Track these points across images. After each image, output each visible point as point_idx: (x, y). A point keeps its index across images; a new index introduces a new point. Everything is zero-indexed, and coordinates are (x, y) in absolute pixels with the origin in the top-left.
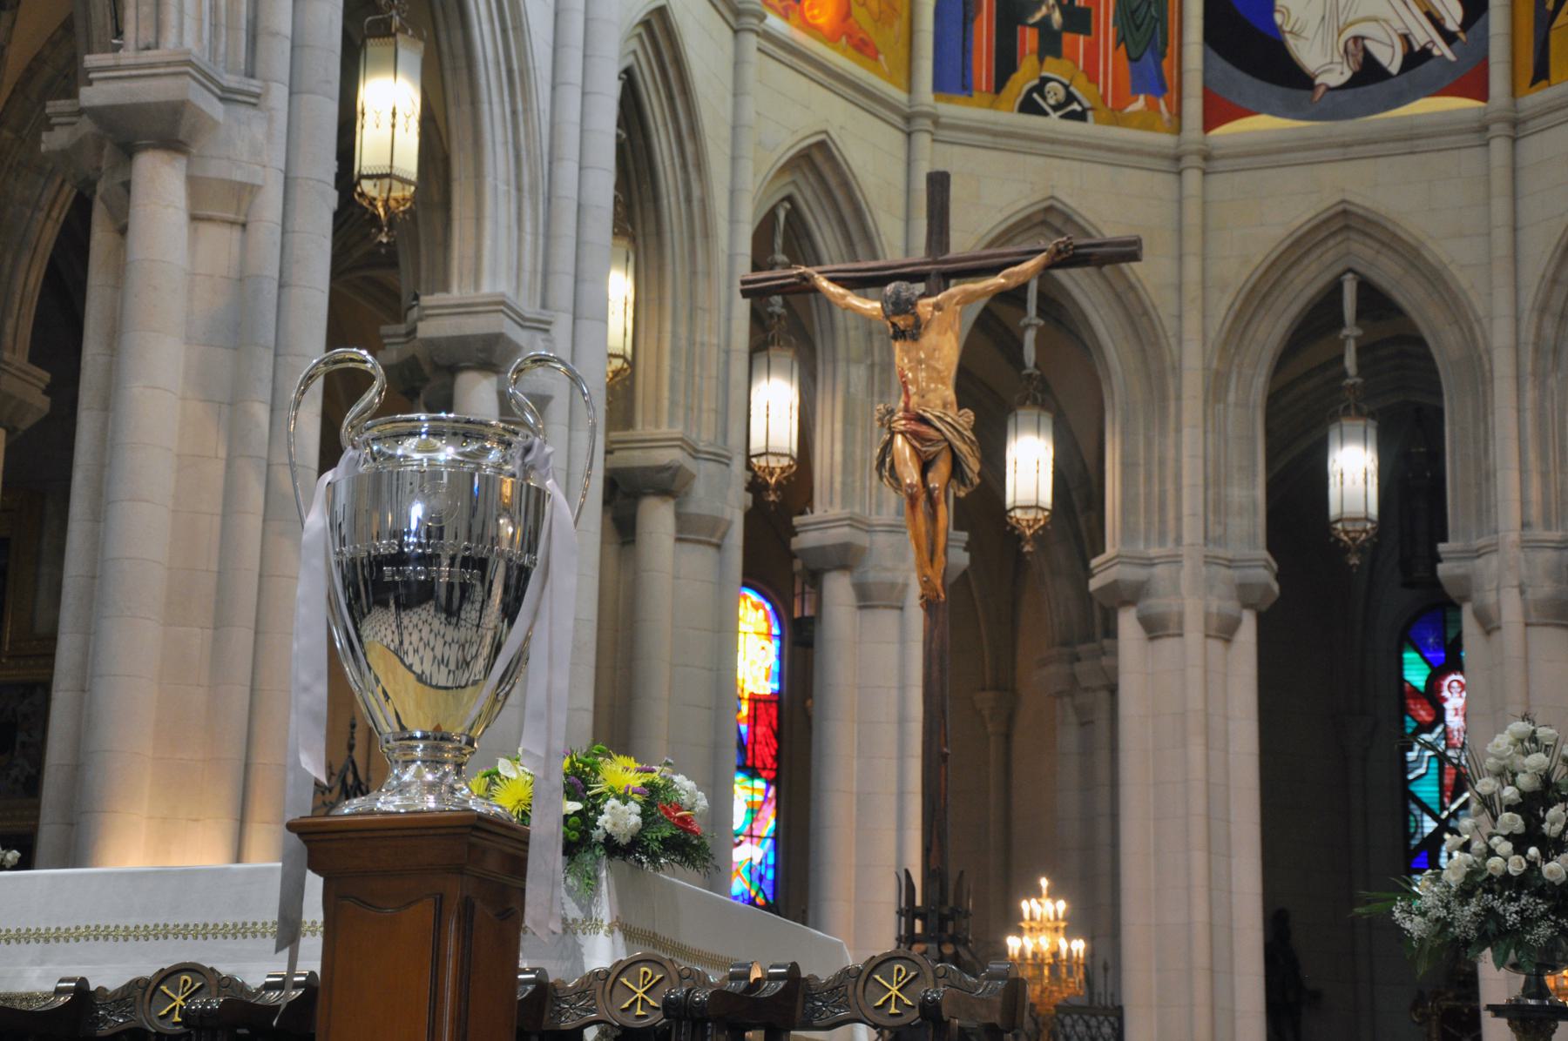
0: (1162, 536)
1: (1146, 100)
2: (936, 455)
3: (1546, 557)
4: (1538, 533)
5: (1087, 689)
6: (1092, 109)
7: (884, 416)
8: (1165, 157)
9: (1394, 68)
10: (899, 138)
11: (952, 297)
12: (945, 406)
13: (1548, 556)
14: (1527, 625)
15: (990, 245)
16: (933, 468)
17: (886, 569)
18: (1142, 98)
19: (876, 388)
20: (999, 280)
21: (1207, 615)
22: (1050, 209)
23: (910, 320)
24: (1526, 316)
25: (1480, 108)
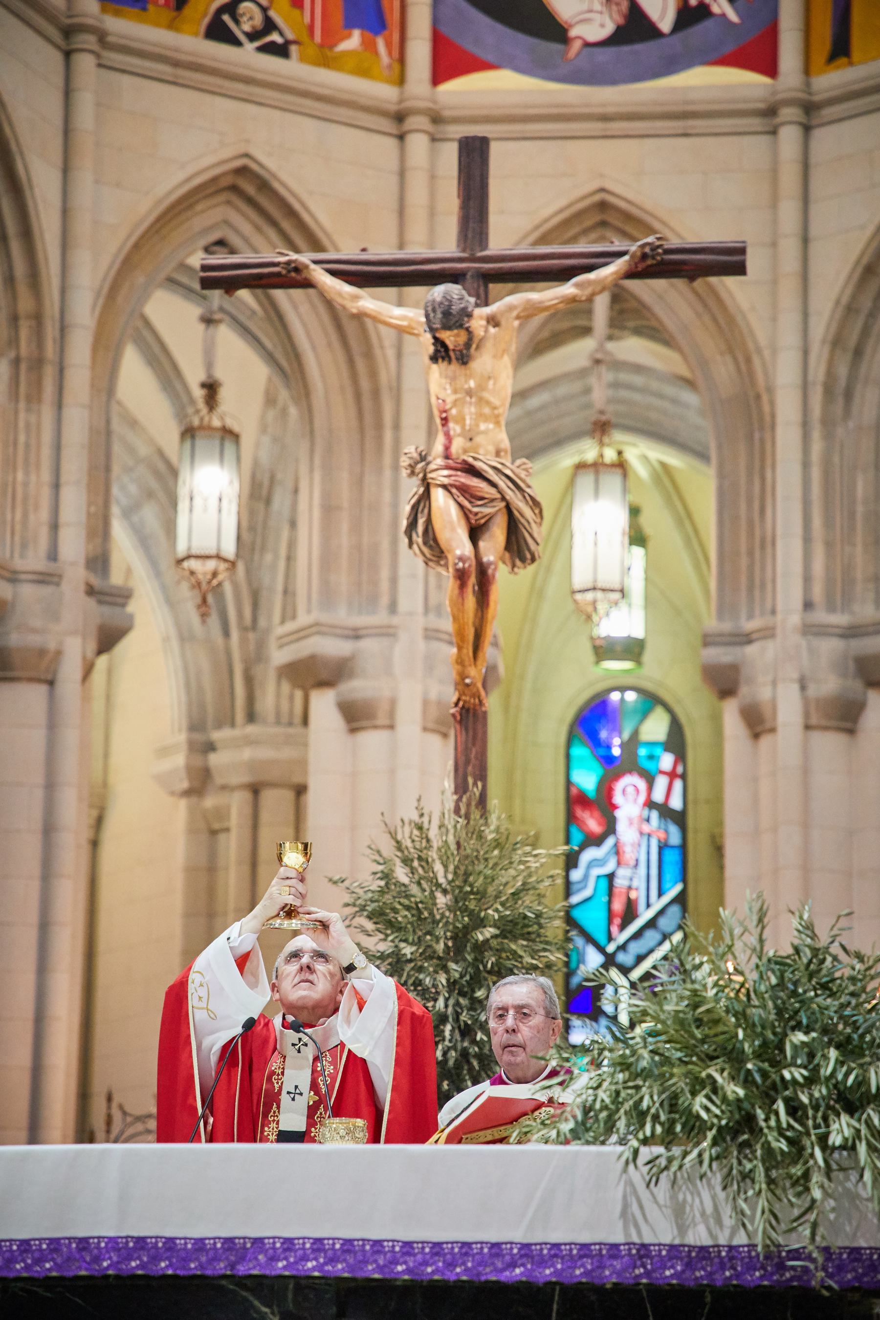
0: (373, 600)
1: (362, 36)
2: (490, 518)
3: (830, 646)
4: (821, 616)
5: (224, 788)
6: (295, 42)
7: (417, 463)
8: (382, 113)
9: (666, 25)
10: (57, 57)
11: (511, 308)
12: (498, 454)
13: (830, 646)
14: (808, 727)
15: (543, 240)
16: (486, 536)
17: (34, 631)
18: (356, 34)
19: (23, 389)
20: (568, 289)
21: (426, 703)
22: (242, 171)
23: (463, 338)
24: (816, 348)
25: (765, 85)
